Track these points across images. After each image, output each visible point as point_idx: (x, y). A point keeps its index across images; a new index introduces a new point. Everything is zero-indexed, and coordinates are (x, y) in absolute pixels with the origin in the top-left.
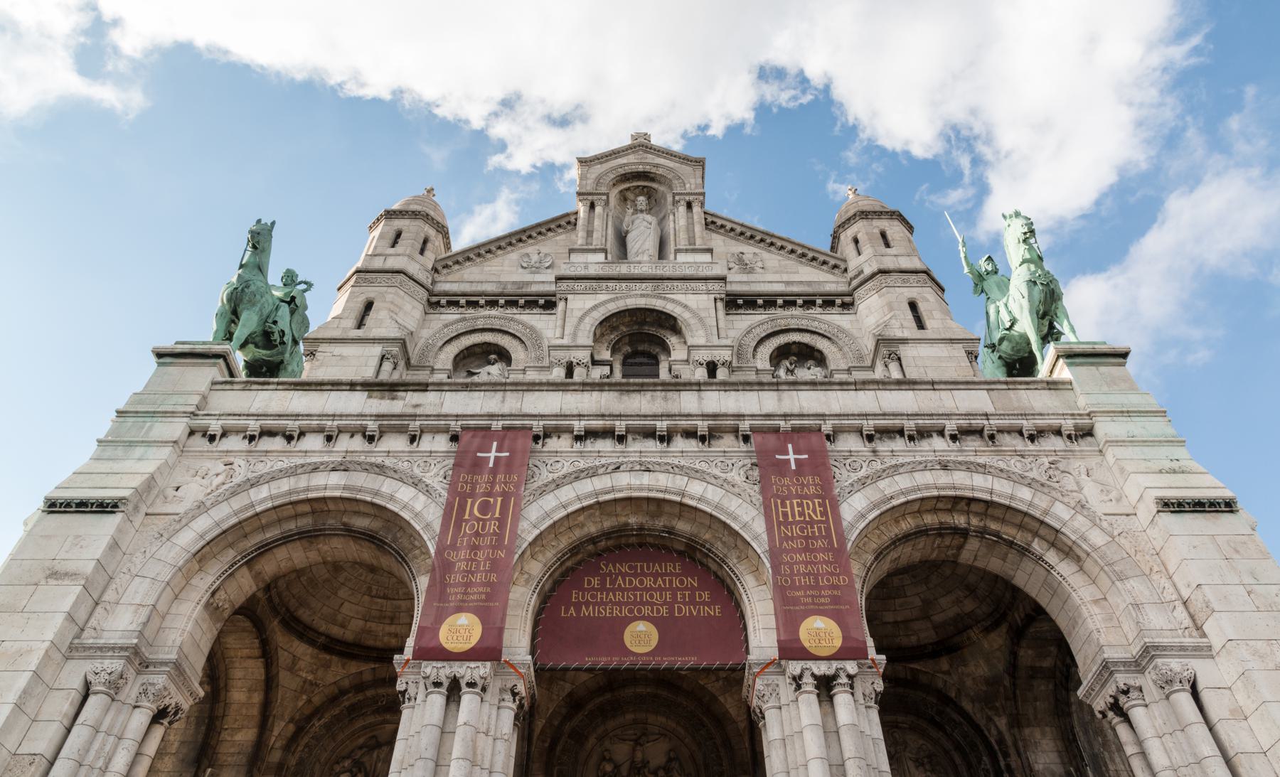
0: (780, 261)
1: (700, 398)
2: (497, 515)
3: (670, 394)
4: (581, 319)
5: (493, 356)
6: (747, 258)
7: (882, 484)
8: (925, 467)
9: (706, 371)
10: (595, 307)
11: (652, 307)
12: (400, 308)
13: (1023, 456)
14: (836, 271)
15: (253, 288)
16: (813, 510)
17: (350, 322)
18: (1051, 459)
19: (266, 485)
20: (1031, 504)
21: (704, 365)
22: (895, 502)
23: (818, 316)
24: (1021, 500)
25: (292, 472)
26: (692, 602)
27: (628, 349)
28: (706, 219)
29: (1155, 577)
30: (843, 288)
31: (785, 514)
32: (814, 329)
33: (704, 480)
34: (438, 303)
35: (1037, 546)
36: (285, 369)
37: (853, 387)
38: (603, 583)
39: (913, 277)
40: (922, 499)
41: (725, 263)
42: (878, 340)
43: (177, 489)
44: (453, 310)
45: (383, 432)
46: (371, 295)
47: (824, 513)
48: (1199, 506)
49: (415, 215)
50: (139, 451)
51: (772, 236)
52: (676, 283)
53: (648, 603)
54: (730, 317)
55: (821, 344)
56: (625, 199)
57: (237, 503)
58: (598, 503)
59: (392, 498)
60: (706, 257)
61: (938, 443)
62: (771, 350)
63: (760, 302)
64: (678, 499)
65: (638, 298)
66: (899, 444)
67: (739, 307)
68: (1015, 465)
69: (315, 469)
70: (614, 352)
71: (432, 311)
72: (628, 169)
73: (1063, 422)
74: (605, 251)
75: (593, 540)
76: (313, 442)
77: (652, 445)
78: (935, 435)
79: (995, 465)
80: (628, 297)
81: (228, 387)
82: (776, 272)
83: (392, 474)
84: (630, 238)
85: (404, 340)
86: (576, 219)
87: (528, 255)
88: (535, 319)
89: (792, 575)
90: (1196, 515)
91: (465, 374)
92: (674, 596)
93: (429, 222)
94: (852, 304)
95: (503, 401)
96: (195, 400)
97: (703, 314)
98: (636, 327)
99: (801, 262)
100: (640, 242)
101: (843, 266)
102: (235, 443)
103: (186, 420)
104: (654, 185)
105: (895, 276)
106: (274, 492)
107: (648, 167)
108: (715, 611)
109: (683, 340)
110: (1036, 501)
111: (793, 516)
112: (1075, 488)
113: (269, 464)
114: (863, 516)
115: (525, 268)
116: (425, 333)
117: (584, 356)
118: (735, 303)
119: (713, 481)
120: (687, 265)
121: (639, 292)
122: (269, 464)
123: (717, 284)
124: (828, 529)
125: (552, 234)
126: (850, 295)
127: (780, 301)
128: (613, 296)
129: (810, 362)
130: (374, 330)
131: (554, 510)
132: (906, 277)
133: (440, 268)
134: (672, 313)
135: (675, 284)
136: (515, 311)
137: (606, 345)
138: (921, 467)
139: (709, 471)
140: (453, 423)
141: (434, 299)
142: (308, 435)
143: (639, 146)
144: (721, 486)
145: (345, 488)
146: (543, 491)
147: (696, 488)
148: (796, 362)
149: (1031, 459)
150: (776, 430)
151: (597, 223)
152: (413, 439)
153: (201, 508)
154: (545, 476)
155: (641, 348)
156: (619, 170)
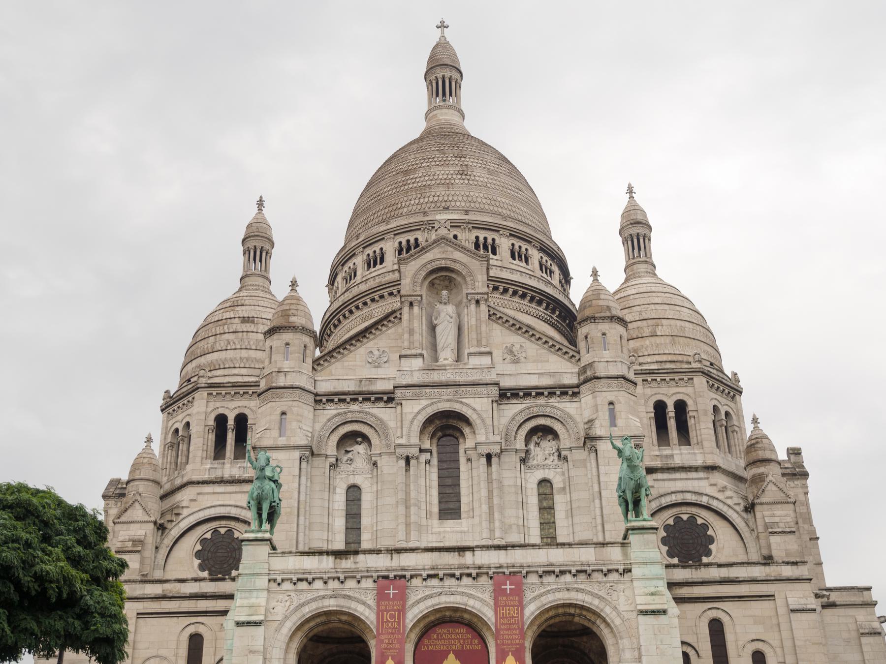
0: (537, 350)
1: (474, 555)
2: (397, 620)
3: (461, 553)
4: (412, 422)
5: (359, 439)
6: (516, 348)
7: (543, 599)
8: (560, 590)
9: (485, 459)
10: (419, 412)
11: (454, 410)
12: (302, 416)
13: (600, 583)
14: (573, 360)
15: (266, 491)
16: (513, 612)
17: (275, 433)
18: (611, 584)
19: (307, 606)
20: (597, 607)
21: (485, 456)
22: (546, 607)
23: (555, 404)
24: (594, 605)
25: (314, 600)
26: (471, 644)
27: (440, 434)
28: (489, 311)
29: (632, 638)
30: (574, 381)
31: (503, 613)
32: (553, 415)
33: (474, 598)
34: (321, 400)
35: (598, 622)
36: (276, 513)
37: (538, 547)
38: (438, 636)
39: (615, 381)
40: (557, 604)
41: (501, 355)
42: (585, 438)
43: (274, 609)
44: (330, 406)
45: (345, 578)
46: (284, 409)
47: (518, 613)
48: (653, 612)
49: (293, 328)
50: (255, 594)
51: (534, 329)
52: (469, 389)
53: (454, 644)
54: (502, 407)
55: (557, 427)
56: (433, 285)
57: (299, 614)
58: (434, 610)
59: (356, 610)
60: (486, 360)
61: (568, 578)
62: (526, 432)
63: (521, 394)
64: (464, 607)
65: (444, 402)
66: (551, 579)
67: (509, 398)
68: (595, 589)
69: (323, 597)
70: (432, 437)
71: (318, 407)
72: (434, 265)
73: (619, 567)
74: (422, 355)
75: (432, 622)
76: (318, 584)
77: (453, 581)
78: (567, 573)
79: (588, 589)
80: (440, 402)
81: (275, 555)
82: (534, 361)
83: (353, 599)
84: (438, 330)
85: (311, 446)
86: (401, 314)
87: (371, 352)
88: (381, 412)
89: (503, 639)
90: (652, 616)
91: (344, 452)
92: (464, 643)
93: (305, 332)
94: (579, 393)
95: (392, 559)
96: (266, 566)
97: (484, 416)
98: (444, 420)
99: (551, 351)
100: (445, 337)
101: (577, 358)
102: (287, 586)
103: (267, 577)
104: (454, 275)
105: (604, 381)
106: (311, 609)
107: (448, 262)
108: (479, 647)
109: (473, 430)
110: (600, 606)
111: (506, 615)
112: (616, 599)
113: (305, 595)
114: (533, 613)
115: (369, 362)
116: (318, 427)
117: (415, 451)
118: (506, 395)
119: (478, 599)
120: (475, 371)
121: (445, 397)
122: (305, 595)
123: (493, 389)
124: (518, 620)
125: (386, 328)
126: (578, 386)
127: (534, 393)
128: (429, 402)
129: (550, 437)
130: (292, 439)
131: (418, 614)
132: (610, 382)
133: (316, 367)
134: (466, 415)
135: (468, 389)
136: (369, 405)
137: (427, 435)
138: (559, 590)
139: (476, 594)
140: (374, 574)
141: (318, 398)
142: (316, 580)
143: (442, 239)
144: (481, 601)
145: (337, 606)
146: (413, 605)
147: (471, 602)
148: (541, 436)
149: (603, 584)
150: (504, 573)
151: (416, 324)
152: (359, 582)
153: (286, 618)
154: (412, 599)
155: (448, 432)
156: (429, 266)
